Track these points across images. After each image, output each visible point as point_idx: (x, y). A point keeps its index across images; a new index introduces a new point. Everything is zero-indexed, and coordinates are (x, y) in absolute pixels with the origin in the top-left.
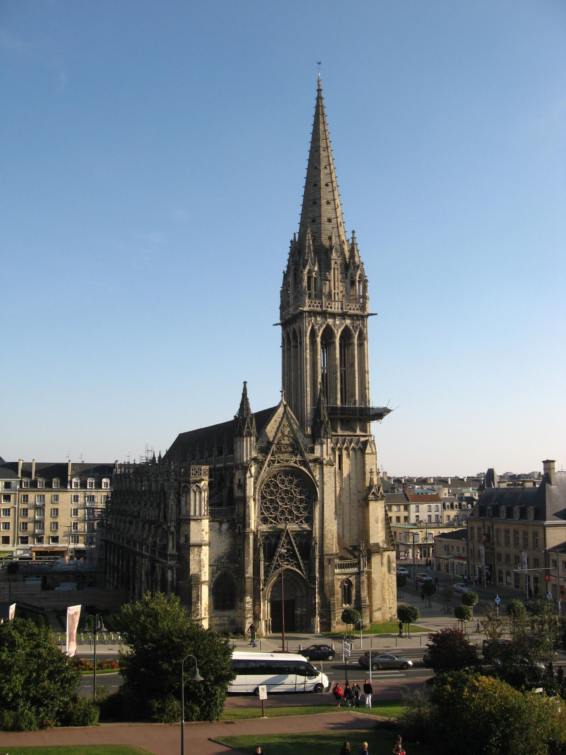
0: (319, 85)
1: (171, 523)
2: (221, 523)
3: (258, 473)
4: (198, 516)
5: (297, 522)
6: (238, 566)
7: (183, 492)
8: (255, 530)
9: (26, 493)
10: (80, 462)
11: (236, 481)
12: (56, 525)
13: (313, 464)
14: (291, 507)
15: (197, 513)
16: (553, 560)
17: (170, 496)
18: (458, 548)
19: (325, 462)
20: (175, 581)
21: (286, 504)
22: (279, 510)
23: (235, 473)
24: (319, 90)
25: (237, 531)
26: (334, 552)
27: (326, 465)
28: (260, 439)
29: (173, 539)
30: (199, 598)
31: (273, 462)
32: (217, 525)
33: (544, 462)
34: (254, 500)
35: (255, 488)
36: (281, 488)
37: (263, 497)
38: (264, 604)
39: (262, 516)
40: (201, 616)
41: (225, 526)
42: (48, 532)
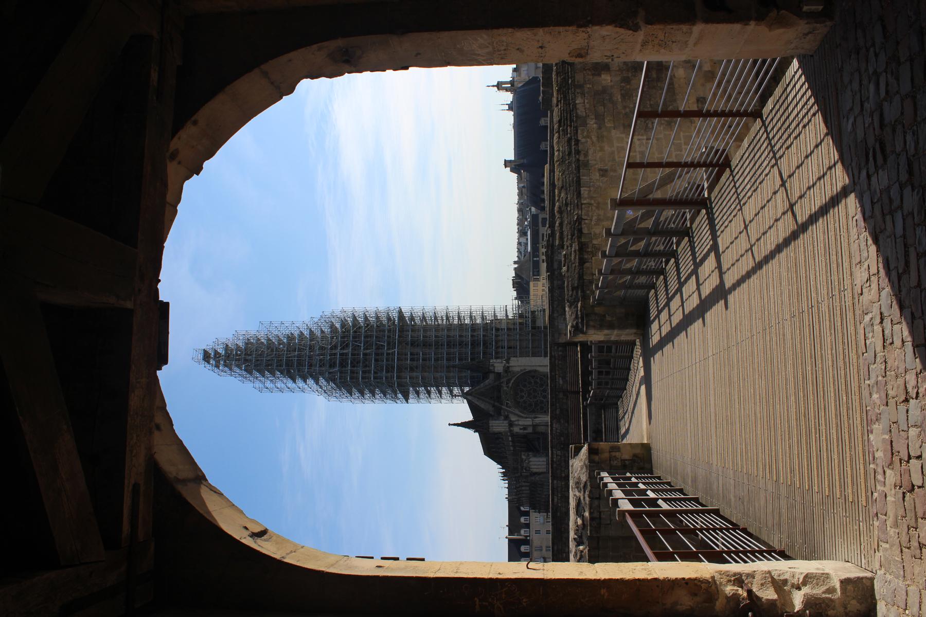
4: (547, 460)
7: (530, 471)
10: (508, 528)
11: (522, 431)
13: (509, 374)
15: (545, 459)
17: (532, 480)
19: (507, 365)
21: (538, 394)
27: (509, 363)
28: (491, 413)
31: (507, 404)
34: (536, 418)
35: (526, 418)
36: (527, 398)
37: (533, 411)
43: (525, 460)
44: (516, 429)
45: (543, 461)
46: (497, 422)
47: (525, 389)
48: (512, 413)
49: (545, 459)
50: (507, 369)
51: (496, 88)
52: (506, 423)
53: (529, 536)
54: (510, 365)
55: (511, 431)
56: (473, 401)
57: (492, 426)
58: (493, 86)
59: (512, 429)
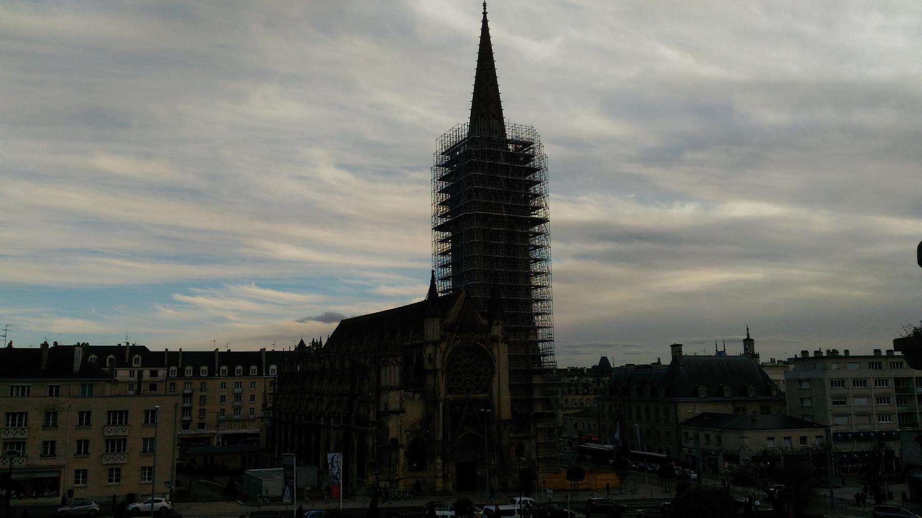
0: (485, 9)
1: (372, 393)
2: (414, 392)
3: (447, 349)
5: (477, 391)
6: (428, 431)
8: (443, 399)
9: (174, 381)
11: (426, 356)
12: (203, 411)
13: (489, 342)
14: (473, 378)
15: (397, 384)
16: (684, 433)
18: (589, 425)
20: (375, 446)
22: (463, 382)
23: (425, 350)
24: (485, 13)
25: (429, 399)
26: (509, 418)
28: (446, 320)
29: (374, 408)
30: (397, 461)
31: (458, 339)
32: (411, 394)
33: (672, 346)
35: (443, 362)
38: (452, 465)
39: (449, 387)
40: (399, 476)
41: (418, 396)
42: (196, 420)
43: (396, 360)
44: (429, 350)
45: (395, 381)
46: (438, 327)
47: (473, 360)
48: (448, 344)
49: (397, 384)
50: (495, 339)
51: (746, 337)
52: (437, 338)
53: (219, 376)
54: (500, 344)
55: (427, 343)
56: (458, 300)
57: (434, 321)
58: (748, 335)
59: (431, 344)
